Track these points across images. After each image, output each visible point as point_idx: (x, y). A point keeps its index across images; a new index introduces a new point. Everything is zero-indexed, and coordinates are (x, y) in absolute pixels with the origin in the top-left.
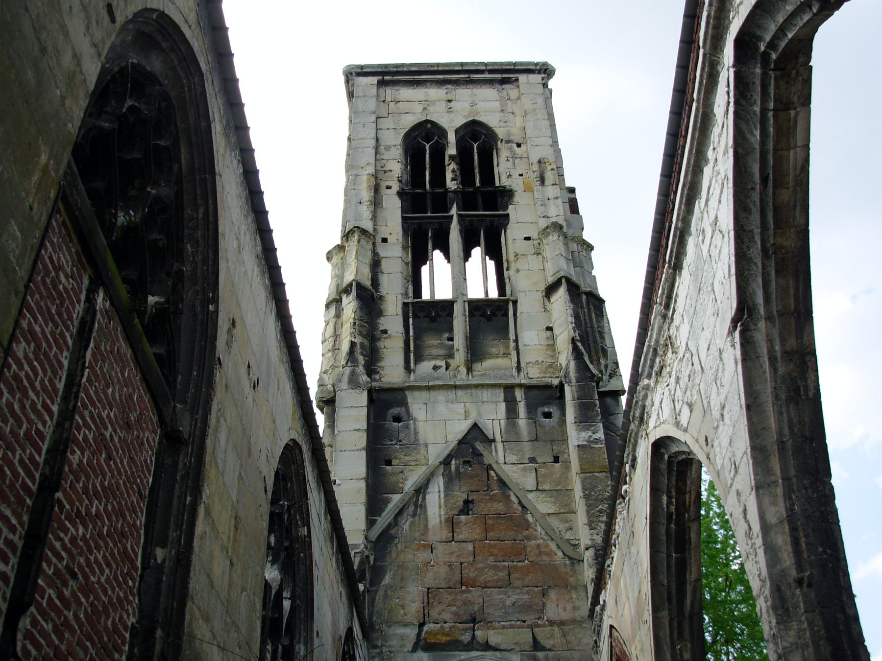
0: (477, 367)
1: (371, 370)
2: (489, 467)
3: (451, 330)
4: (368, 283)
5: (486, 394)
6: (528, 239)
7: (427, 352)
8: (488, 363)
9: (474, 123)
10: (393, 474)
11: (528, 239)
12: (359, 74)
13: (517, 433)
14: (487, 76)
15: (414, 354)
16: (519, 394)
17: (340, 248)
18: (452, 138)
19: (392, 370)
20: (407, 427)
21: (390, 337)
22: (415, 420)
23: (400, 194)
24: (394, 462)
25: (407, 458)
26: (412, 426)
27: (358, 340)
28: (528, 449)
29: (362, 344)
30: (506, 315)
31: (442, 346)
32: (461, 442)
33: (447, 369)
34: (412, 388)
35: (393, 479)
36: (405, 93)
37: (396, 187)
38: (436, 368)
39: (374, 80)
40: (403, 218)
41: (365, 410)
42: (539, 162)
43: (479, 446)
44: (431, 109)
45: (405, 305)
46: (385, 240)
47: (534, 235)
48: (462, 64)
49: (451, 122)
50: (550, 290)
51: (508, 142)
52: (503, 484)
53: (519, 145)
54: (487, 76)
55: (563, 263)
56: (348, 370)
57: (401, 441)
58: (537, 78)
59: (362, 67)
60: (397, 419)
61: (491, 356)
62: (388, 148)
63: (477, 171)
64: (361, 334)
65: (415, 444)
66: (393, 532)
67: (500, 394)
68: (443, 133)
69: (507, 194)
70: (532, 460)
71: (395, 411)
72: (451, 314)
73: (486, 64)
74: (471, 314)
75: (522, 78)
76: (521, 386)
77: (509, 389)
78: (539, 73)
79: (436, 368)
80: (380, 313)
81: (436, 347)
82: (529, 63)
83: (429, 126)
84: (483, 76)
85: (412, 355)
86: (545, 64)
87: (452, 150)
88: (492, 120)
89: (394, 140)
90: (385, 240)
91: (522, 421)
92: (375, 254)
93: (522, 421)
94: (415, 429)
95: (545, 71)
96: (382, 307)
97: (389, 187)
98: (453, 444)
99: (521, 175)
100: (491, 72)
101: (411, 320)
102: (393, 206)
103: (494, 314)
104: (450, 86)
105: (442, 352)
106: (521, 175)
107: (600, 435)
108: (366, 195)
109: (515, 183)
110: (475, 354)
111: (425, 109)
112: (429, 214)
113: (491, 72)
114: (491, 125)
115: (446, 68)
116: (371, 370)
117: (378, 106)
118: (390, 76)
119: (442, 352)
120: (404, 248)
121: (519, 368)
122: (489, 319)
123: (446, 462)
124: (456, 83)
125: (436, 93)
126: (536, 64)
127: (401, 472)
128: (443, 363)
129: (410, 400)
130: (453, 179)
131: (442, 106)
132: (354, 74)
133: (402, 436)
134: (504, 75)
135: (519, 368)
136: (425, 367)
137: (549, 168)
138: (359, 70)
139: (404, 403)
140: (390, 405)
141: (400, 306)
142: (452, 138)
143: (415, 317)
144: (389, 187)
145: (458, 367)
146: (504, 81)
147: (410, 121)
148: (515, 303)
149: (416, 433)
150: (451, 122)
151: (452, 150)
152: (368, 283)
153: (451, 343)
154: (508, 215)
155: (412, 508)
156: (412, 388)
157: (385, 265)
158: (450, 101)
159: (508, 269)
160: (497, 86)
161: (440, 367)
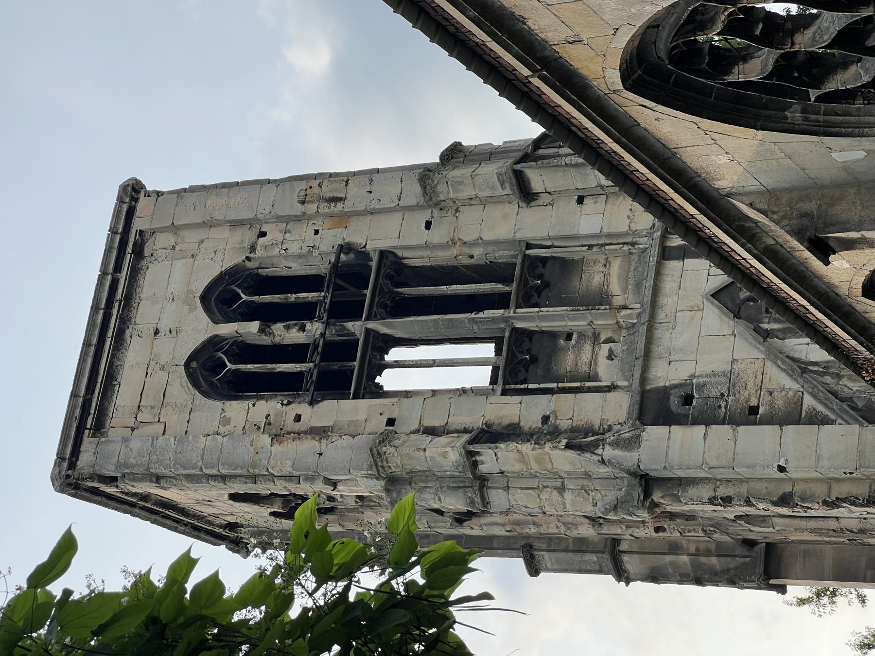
3: (553, 335)
4: (466, 437)
5: (669, 284)
6: (428, 225)
8: (615, 287)
9: (205, 298)
10: (771, 405)
11: (428, 225)
12: (72, 466)
14: (123, 276)
15: (584, 383)
18: (227, 329)
20: (701, 387)
21: (554, 412)
22: (693, 376)
24: (754, 402)
25: (750, 385)
26: (701, 380)
30: (544, 260)
31: (578, 347)
32: (737, 316)
33: (613, 342)
34: (643, 380)
35: (780, 403)
36: (125, 397)
37: (303, 409)
39: (88, 443)
40: (356, 397)
41: (674, 428)
42: (303, 202)
45: (504, 393)
47: (426, 215)
48: (95, 308)
49: (200, 328)
51: (253, 249)
53: (263, 234)
54: (123, 276)
57: (722, 395)
58: (143, 204)
59: (60, 457)
60: (688, 400)
61: (606, 283)
62: (225, 421)
63: (293, 297)
65: (731, 378)
66: (860, 404)
67: (673, 266)
68: (214, 343)
72: (529, 334)
75: (138, 224)
76: (664, 238)
78: (136, 200)
79: (611, 356)
81: (578, 355)
83: (194, 364)
84: (122, 281)
85: (588, 384)
86: (124, 188)
94: (707, 376)
95: (132, 192)
96: (506, 422)
97: (298, 418)
98: (740, 327)
99: (317, 232)
100: (118, 268)
101: (531, 386)
104: (128, 332)
105: (588, 348)
106: (317, 232)
109: (330, 239)
110: (599, 299)
111: (162, 368)
112: (356, 364)
113: (118, 268)
114: (216, 272)
115: (97, 332)
118: (89, 414)
119: (588, 348)
124: (124, 321)
125: (135, 355)
126: (120, 200)
127: (771, 393)
128: (605, 348)
129: (662, 384)
130: (303, 329)
133: (714, 393)
136: (606, 371)
137: (316, 190)
138: (65, 464)
139: (665, 392)
141: (507, 399)
142: (227, 329)
143: (524, 381)
144: (298, 418)
145: (617, 323)
146: (139, 252)
147: (180, 389)
148: (529, 246)
149: (714, 375)
150: (200, 328)
151: (250, 330)
152: (466, 437)
153: (575, 337)
154: (383, 254)
155: (828, 379)
156: (643, 380)
158: (157, 332)
159: (472, 257)
160: (143, 263)
161: (611, 351)
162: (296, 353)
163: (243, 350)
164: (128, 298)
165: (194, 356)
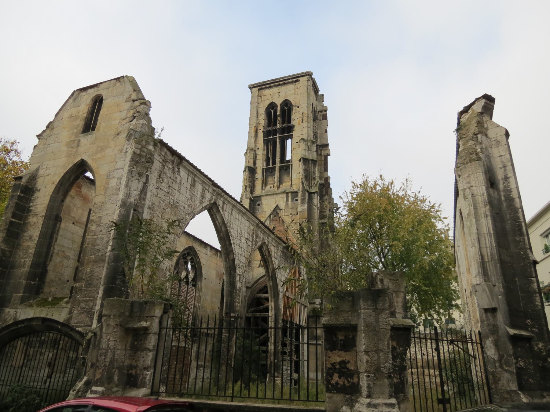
0: (281, 186)
1: (252, 192)
2: (280, 217)
5: (281, 196)
7: (269, 183)
8: (284, 184)
9: (286, 100)
12: (253, 87)
13: (288, 206)
14: (291, 80)
15: (265, 183)
16: (290, 195)
17: (246, 153)
18: (279, 108)
19: (258, 191)
23: (263, 132)
27: (248, 184)
28: (290, 211)
29: (249, 185)
32: (273, 210)
38: (271, 187)
39: (257, 89)
40: (264, 140)
43: (278, 211)
44: (274, 97)
45: (263, 169)
46: (258, 149)
48: (283, 78)
50: (300, 160)
52: (283, 222)
54: (291, 80)
55: (304, 152)
56: (245, 194)
58: (306, 78)
59: (253, 85)
60: (259, 205)
64: (249, 182)
67: (285, 195)
69: (293, 126)
70: (291, 214)
71: (258, 203)
73: (289, 76)
74: (280, 170)
75: (301, 79)
77: (287, 193)
80: (256, 173)
82: (303, 73)
86: (308, 72)
87: (278, 113)
88: (290, 99)
89: (262, 111)
90: (258, 149)
91: (290, 203)
92: (256, 154)
93: (290, 203)
102: (261, 135)
103: (286, 169)
107: (306, 207)
108: (253, 134)
110: (280, 182)
113: (292, 78)
116: (252, 192)
117: (258, 99)
118: (261, 87)
120: (264, 150)
121: (291, 186)
122: (286, 170)
123: (270, 216)
124: (281, 85)
125: (275, 90)
126: (305, 73)
131: (277, 95)
132: (251, 87)
134: (295, 79)
135: (291, 186)
136: (268, 187)
139: (260, 200)
140: (257, 201)
142: (279, 108)
143: (266, 172)
146: (296, 81)
147: (267, 103)
150: (279, 102)
152: (251, 165)
157: (258, 157)
160: (294, 83)
162: (275, 124)
163: (276, 112)
164: (286, 84)
165: (275, 103)
